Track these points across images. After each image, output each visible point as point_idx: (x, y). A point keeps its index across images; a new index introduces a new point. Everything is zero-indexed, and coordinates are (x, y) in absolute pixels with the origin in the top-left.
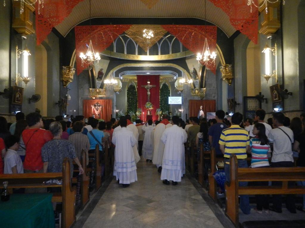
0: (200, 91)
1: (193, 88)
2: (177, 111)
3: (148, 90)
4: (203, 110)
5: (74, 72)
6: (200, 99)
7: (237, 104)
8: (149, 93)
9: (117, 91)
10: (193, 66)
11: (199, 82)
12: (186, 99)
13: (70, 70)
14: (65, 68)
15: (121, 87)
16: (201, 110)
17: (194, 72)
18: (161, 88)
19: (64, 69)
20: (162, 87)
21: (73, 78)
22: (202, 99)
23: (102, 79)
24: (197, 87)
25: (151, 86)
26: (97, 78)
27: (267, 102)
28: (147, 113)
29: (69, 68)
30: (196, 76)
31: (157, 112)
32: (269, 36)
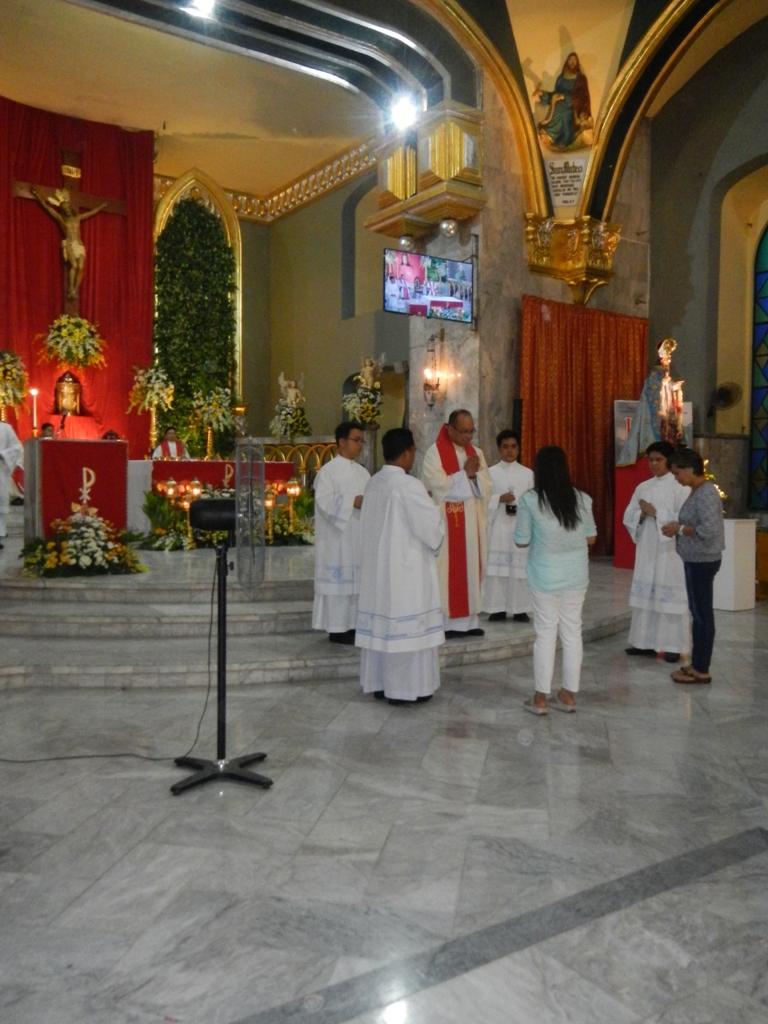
0: (589, 243)
1: (544, 213)
2: (292, 393)
3: (73, 226)
4: (675, 379)
6: (570, 299)
8: (77, 250)
10: (565, 36)
12: (499, 285)
16: (661, 376)
17: (559, 89)
18: (159, 227)
20: (172, 223)
22: (580, 304)
24: (569, 209)
28: (57, 392)
30: (581, 121)
31: (145, 390)
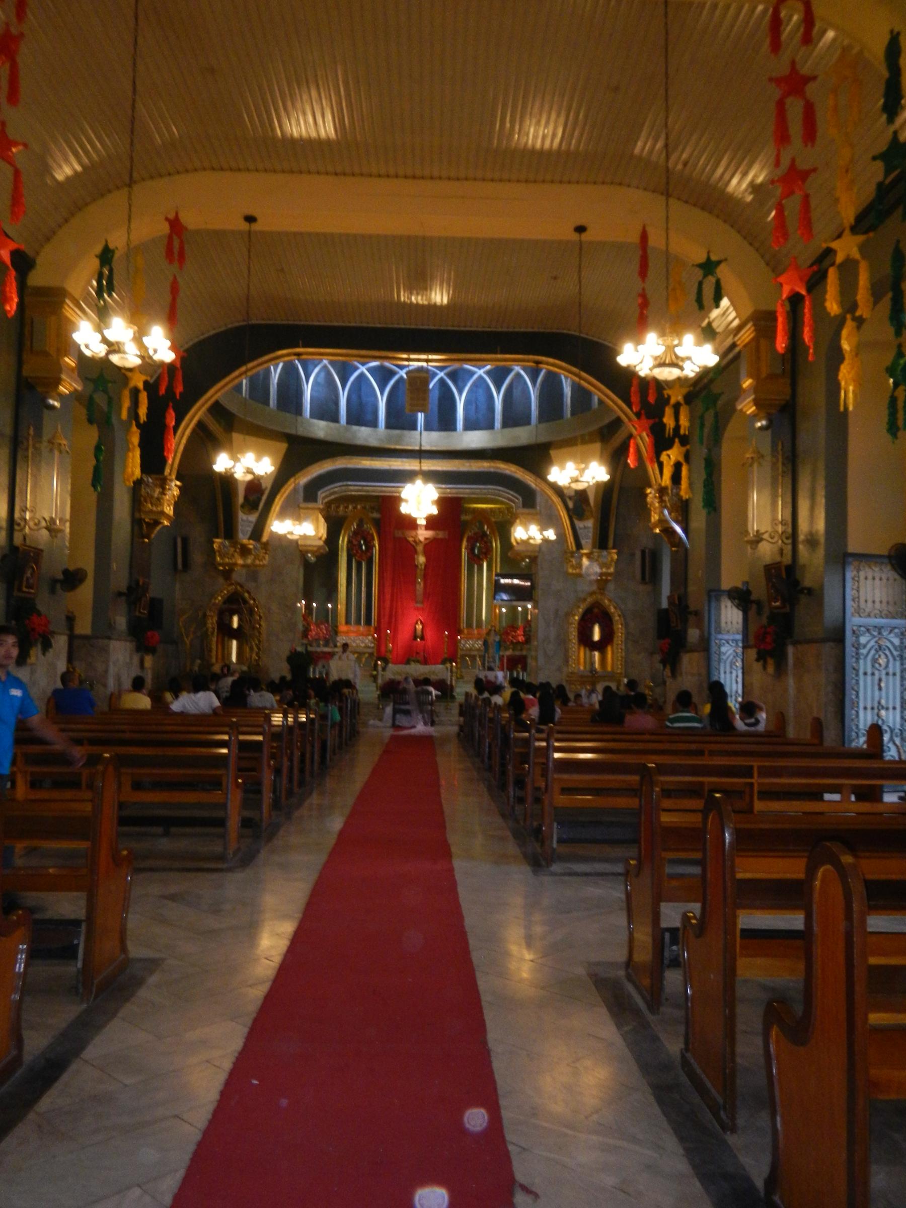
1: (574, 549)
3: (420, 548)
5: (176, 492)
7: (690, 613)
9: (307, 552)
11: (591, 530)
13: (164, 489)
14: (150, 480)
15: (325, 536)
19: (147, 485)
21: (171, 513)
23: (257, 509)
25: (429, 534)
26: (242, 506)
27: (759, 612)
29: (163, 483)
32: (760, 420)
